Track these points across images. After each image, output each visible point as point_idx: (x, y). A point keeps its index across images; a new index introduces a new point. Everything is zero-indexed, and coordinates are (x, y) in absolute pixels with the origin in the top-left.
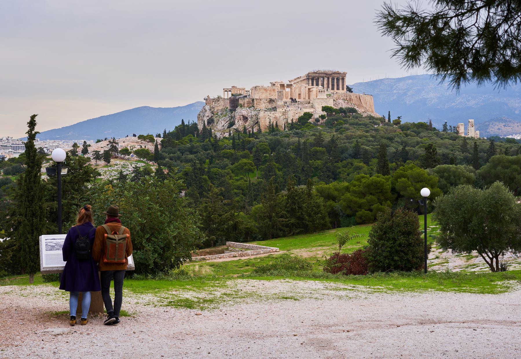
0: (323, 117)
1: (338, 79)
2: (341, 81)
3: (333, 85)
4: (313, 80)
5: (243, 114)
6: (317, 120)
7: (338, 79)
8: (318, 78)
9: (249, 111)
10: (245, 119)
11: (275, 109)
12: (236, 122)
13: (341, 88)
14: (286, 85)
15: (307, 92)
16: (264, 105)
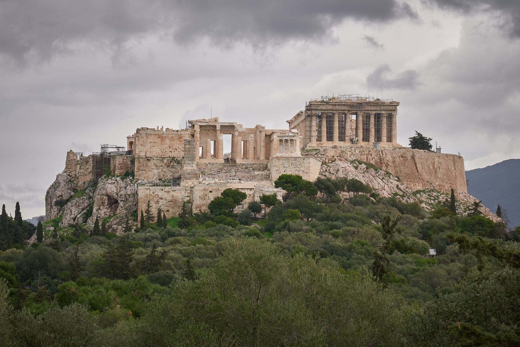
0: (268, 200)
1: (378, 117)
2: (384, 121)
3: (366, 131)
4: (320, 117)
5: (109, 191)
6: (254, 207)
7: (378, 117)
8: (334, 114)
9: (123, 185)
10: (113, 202)
11: (176, 181)
12: (94, 210)
13: (384, 138)
14: (218, 127)
15: (263, 144)
16: (156, 171)
